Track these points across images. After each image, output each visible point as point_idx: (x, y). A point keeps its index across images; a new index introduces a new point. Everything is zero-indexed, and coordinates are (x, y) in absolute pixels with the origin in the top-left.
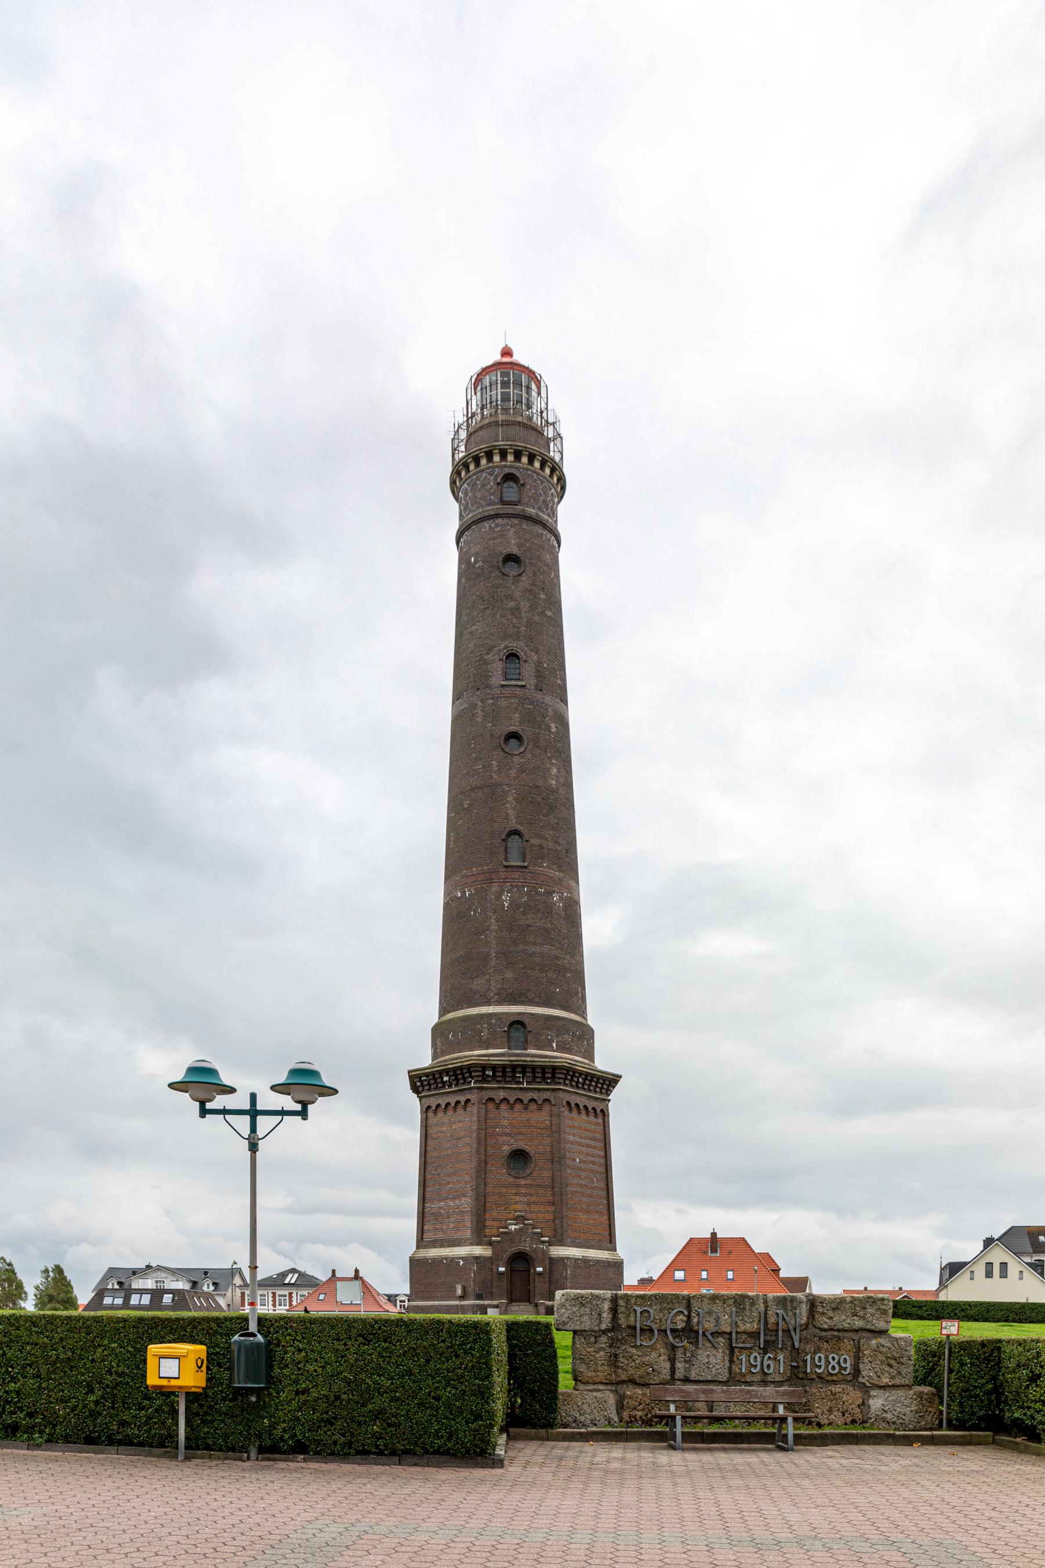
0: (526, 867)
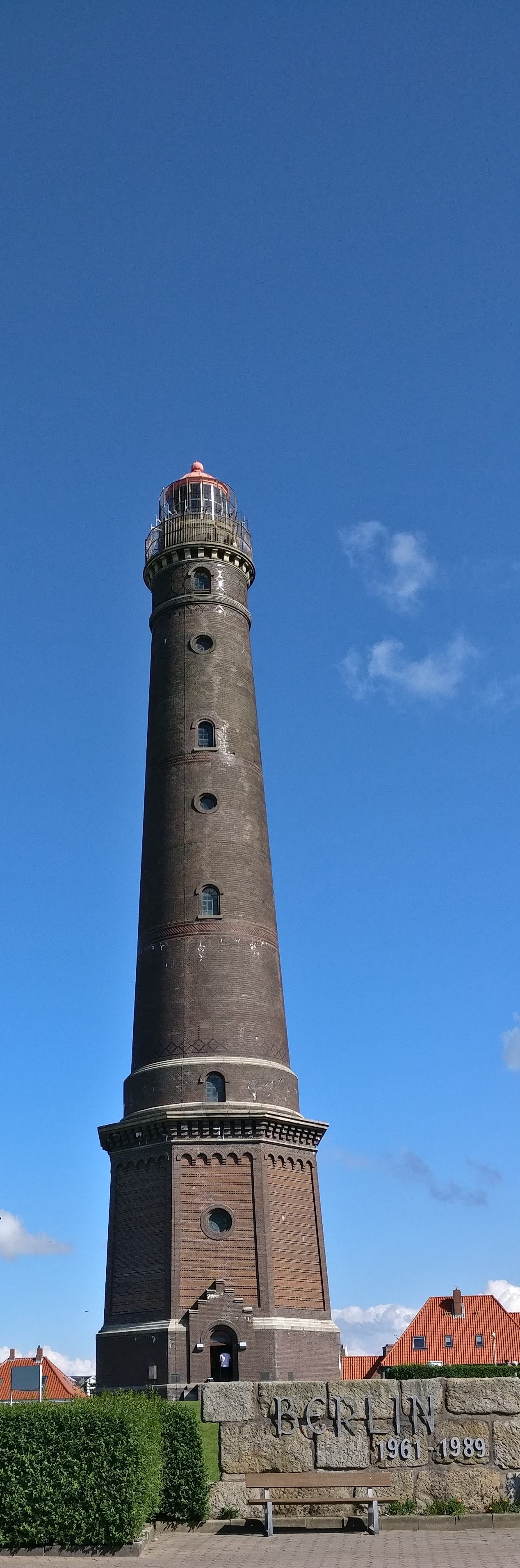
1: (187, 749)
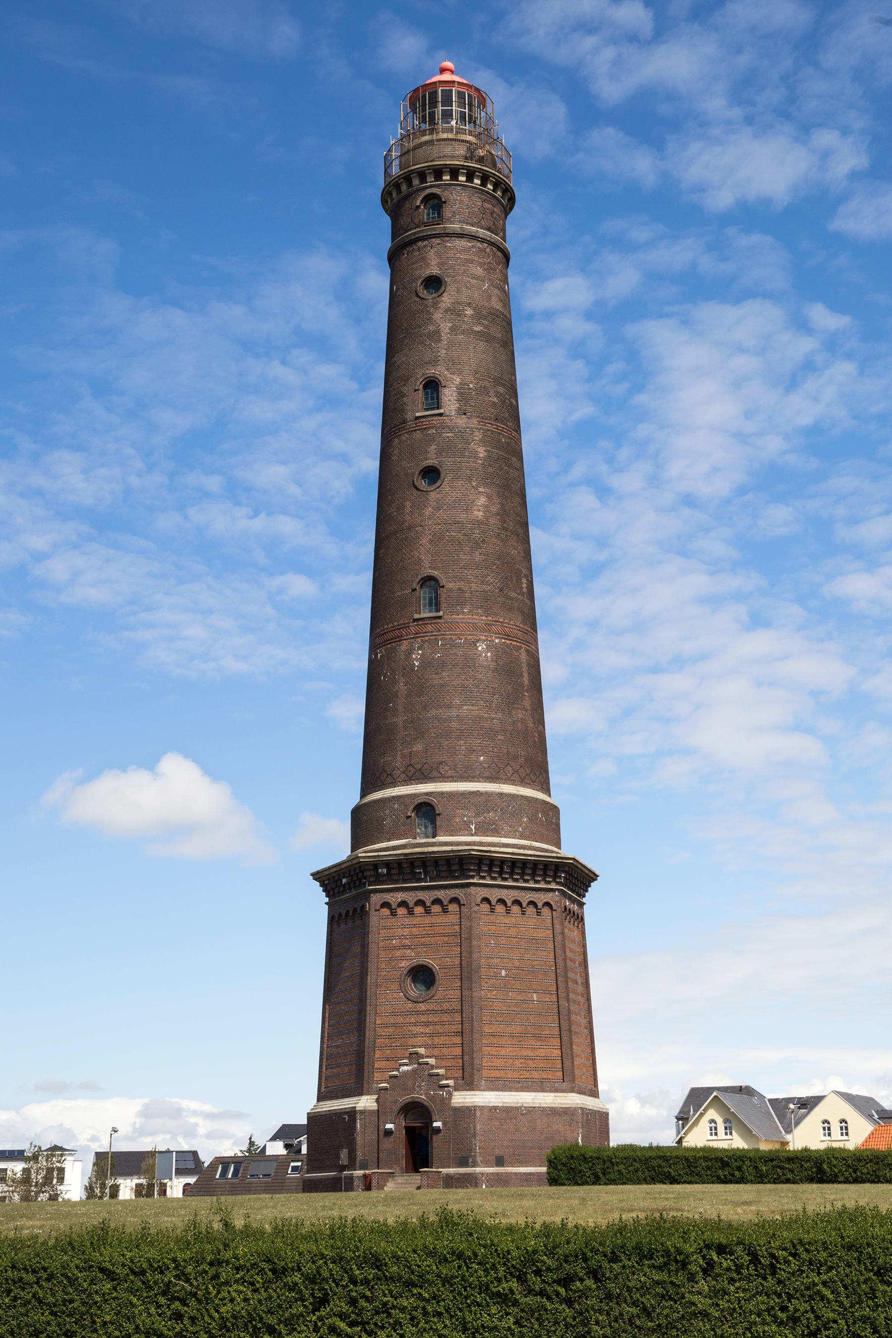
0: (440, 617)
1: (409, 416)
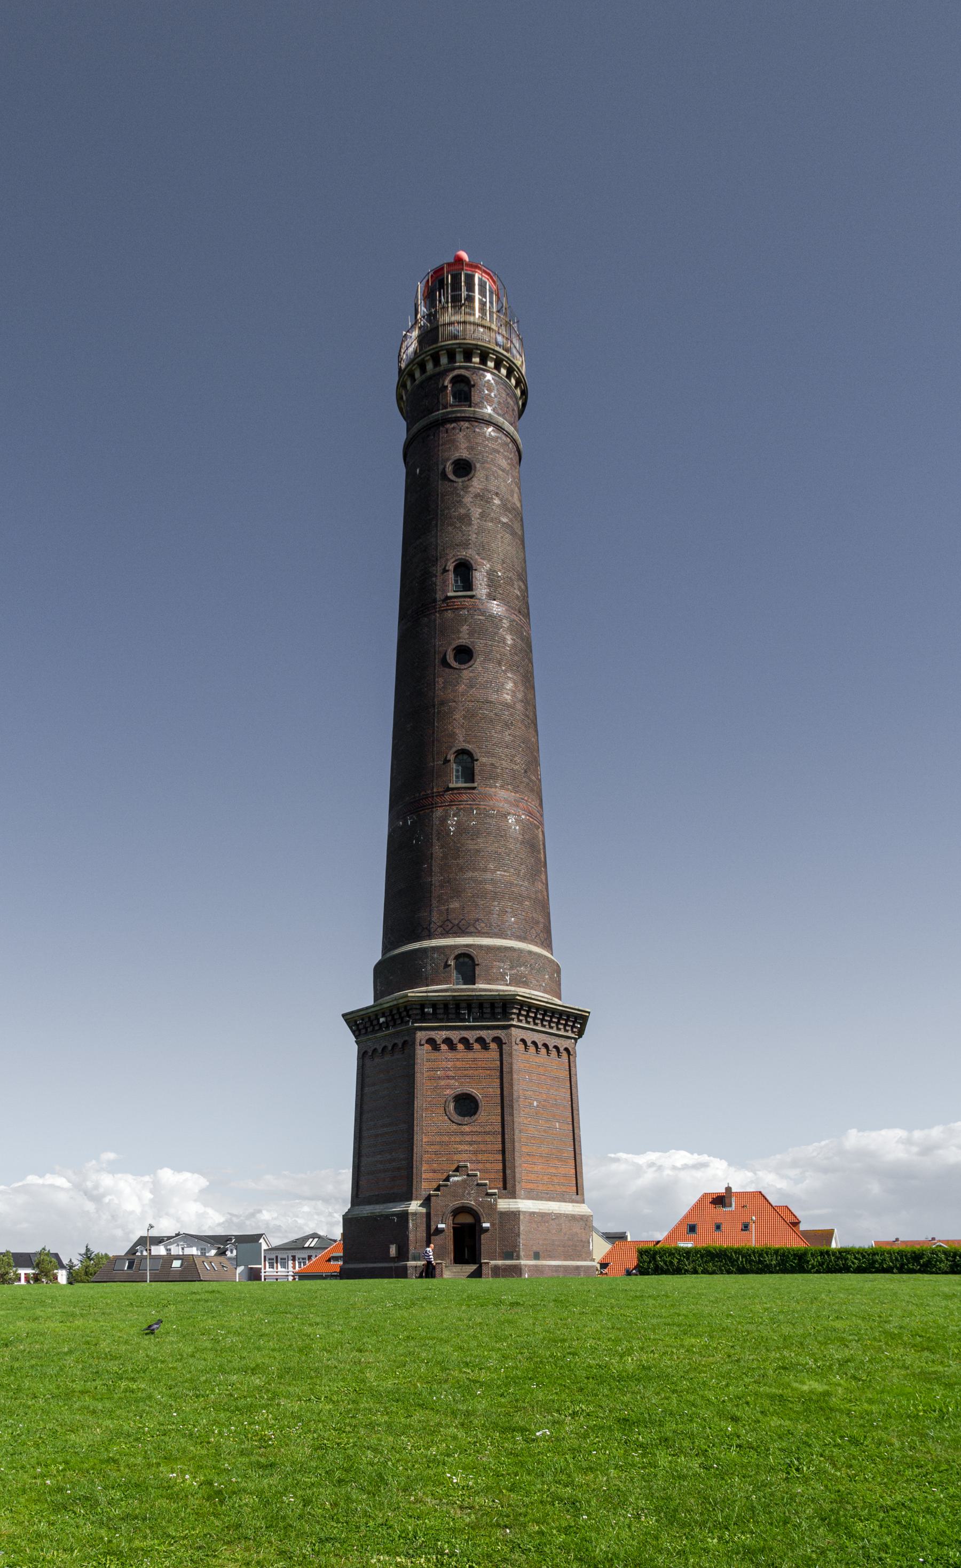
0: (474, 788)
1: (439, 596)
